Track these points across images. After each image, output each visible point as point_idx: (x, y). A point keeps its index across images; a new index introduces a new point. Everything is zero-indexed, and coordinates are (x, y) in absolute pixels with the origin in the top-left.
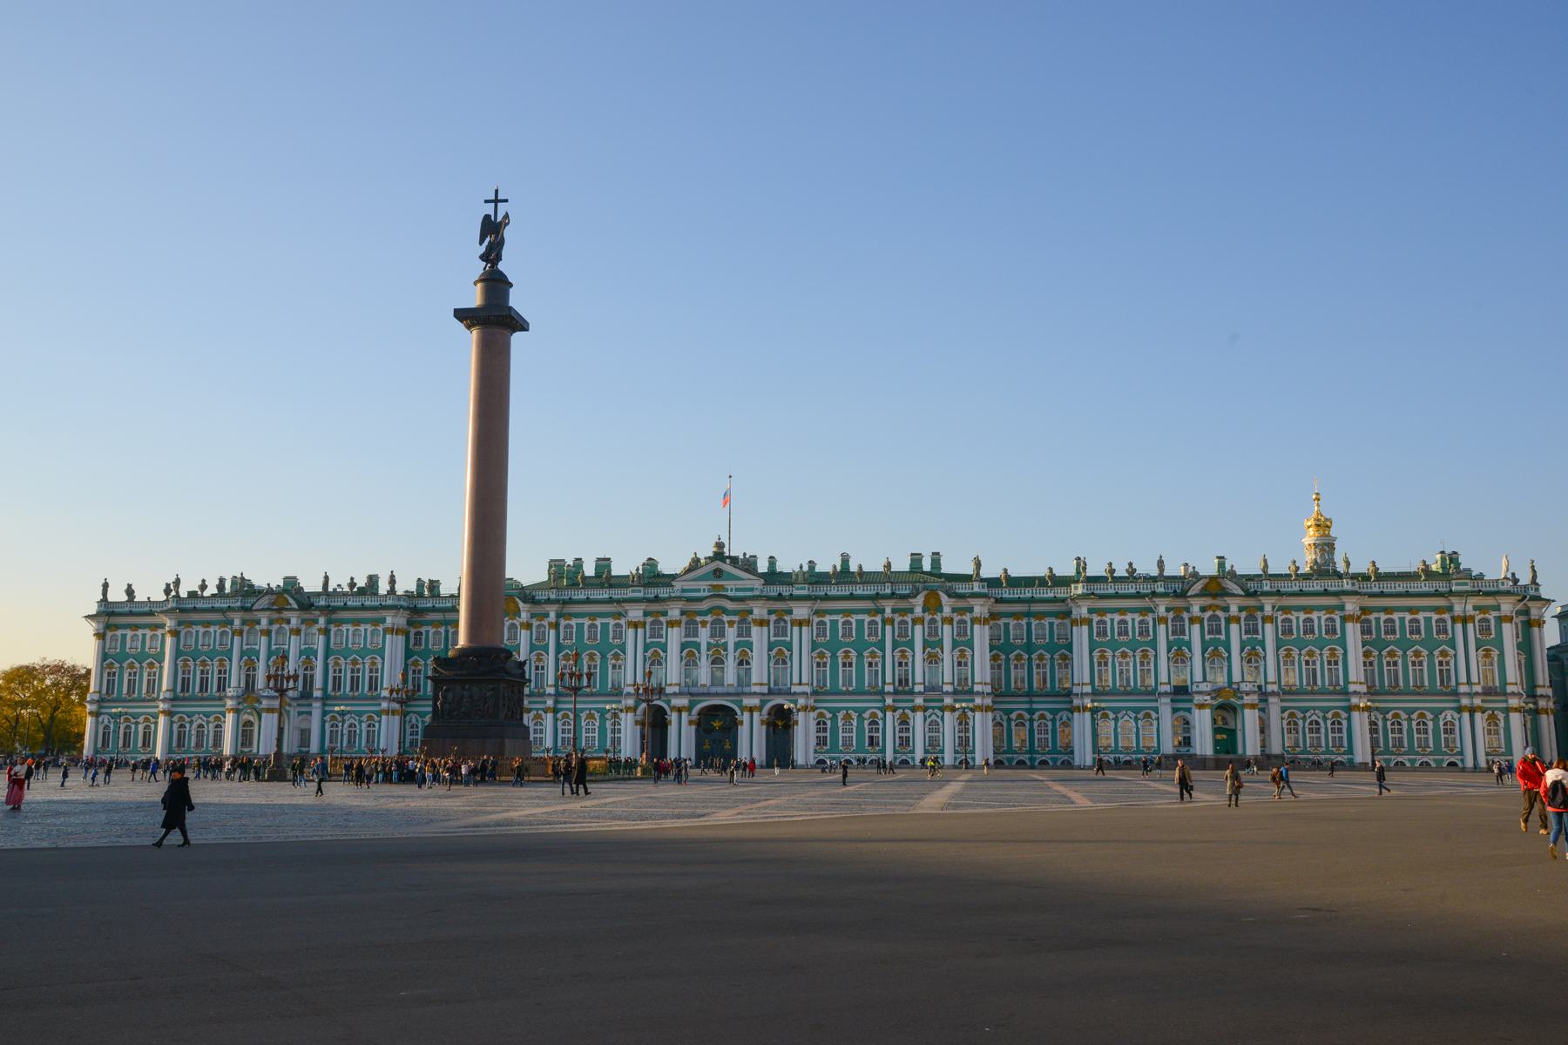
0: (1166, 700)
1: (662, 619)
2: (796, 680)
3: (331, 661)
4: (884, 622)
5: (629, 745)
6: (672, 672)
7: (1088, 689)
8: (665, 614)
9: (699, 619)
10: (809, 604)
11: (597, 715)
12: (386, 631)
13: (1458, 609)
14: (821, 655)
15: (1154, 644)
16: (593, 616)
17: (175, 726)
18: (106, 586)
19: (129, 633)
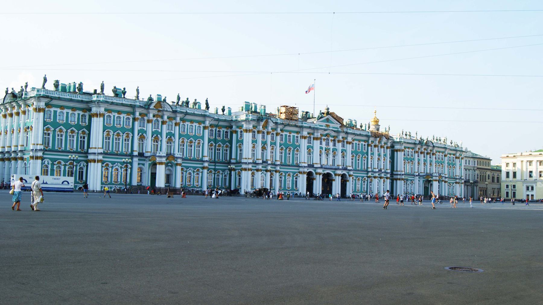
0: (417, 177)
1: (312, 136)
2: (348, 165)
3: (181, 140)
4: (368, 145)
5: (302, 188)
6: (316, 160)
7: (403, 173)
8: (313, 134)
9: (323, 138)
10: (352, 136)
11: (292, 174)
12: (205, 128)
13: (458, 155)
14: (353, 156)
15: (414, 159)
16: (290, 132)
17: (103, 169)
18: (45, 80)
19: (59, 110)
